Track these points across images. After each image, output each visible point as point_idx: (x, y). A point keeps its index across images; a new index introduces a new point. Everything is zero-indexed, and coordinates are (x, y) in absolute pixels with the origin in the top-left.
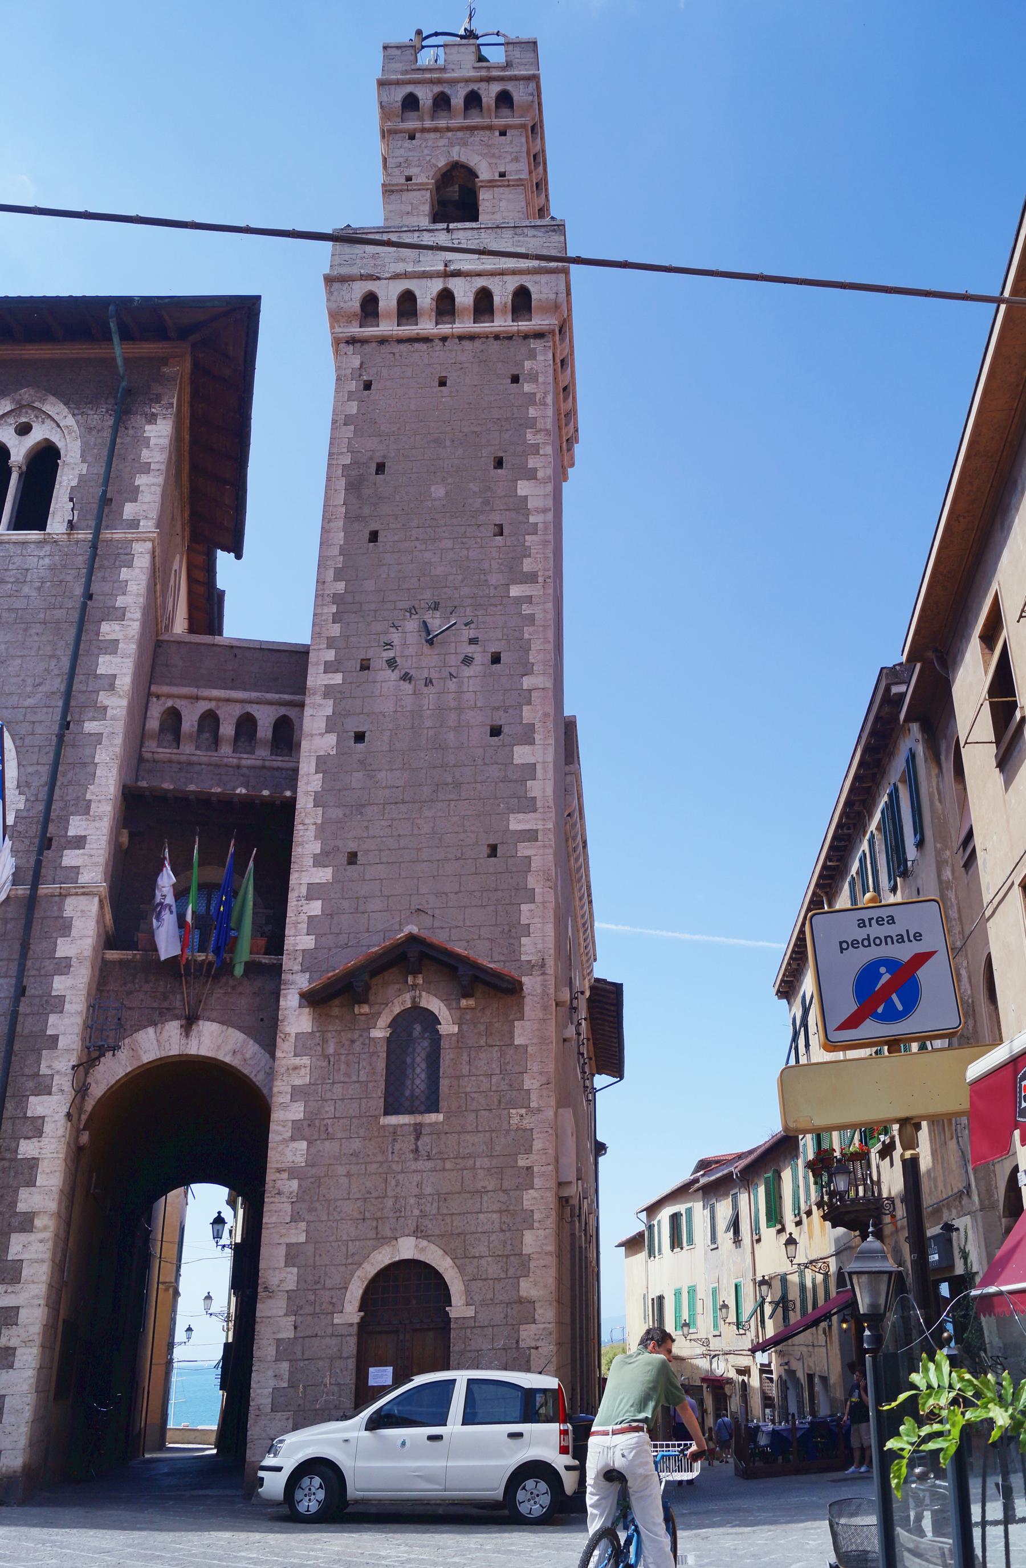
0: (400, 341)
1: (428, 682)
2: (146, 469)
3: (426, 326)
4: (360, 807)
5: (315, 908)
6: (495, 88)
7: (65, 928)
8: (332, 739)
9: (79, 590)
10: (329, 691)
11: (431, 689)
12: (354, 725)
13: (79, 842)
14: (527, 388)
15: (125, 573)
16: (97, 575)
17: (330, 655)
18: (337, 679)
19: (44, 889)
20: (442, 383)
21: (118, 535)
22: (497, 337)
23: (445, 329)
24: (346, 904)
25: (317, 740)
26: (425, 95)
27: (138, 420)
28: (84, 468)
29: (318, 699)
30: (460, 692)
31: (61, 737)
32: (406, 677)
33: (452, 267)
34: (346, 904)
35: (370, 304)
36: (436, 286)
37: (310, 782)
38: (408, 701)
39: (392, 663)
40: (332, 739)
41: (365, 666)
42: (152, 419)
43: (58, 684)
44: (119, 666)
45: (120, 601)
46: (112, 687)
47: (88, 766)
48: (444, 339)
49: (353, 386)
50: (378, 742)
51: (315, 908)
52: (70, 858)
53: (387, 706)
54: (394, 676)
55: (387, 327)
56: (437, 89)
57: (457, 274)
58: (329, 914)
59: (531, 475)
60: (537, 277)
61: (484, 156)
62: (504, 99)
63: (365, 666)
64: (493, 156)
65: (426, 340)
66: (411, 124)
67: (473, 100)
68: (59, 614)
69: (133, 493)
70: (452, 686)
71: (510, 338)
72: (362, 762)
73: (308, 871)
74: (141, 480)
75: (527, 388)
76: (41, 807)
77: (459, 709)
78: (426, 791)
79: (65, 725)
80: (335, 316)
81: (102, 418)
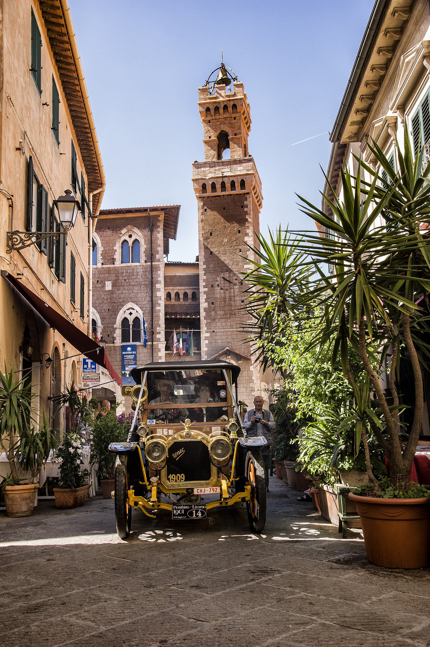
0: (213, 197)
1: (227, 290)
2: (159, 246)
3: (219, 192)
4: (214, 320)
5: (207, 342)
6: (232, 103)
7: (159, 350)
8: (207, 304)
9: (150, 277)
10: (205, 293)
11: (228, 292)
12: (210, 301)
13: (159, 333)
14: (246, 209)
15: (159, 272)
16: (153, 273)
17: (204, 284)
18: (206, 289)
19: (154, 343)
20: (224, 209)
21: (156, 263)
22: (237, 194)
23: (224, 193)
24: (213, 341)
25: (203, 305)
26: (212, 108)
27: (155, 233)
28: (146, 246)
29: (203, 294)
30: (234, 292)
31: (152, 311)
32: (221, 289)
33: (225, 175)
34: (213, 341)
35: (204, 187)
36: (220, 181)
37: (203, 314)
38: (223, 295)
39: (218, 285)
40: (207, 304)
41: (212, 286)
42: (159, 232)
43: (149, 299)
44: (161, 294)
45: (159, 279)
46: (161, 299)
47: (158, 316)
48: (224, 196)
49: (202, 211)
50: (217, 304)
51: (207, 342)
52: (158, 336)
53: (218, 296)
54: (219, 288)
55: (209, 193)
56: (215, 105)
57: (226, 177)
58: (210, 343)
59: (247, 235)
60: (246, 176)
61: (230, 127)
62: (234, 106)
63: (212, 286)
64: (233, 128)
65: (219, 196)
66: (209, 118)
67: (225, 107)
68: (147, 282)
69: (158, 252)
70: (232, 291)
71: (240, 194)
72: (214, 309)
73: (204, 334)
74: (159, 249)
75: (246, 209)
76: (150, 326)
77: (234, 296)
78: (228, 316)
79: (152, 308)
80: (196, 190)
81: (147, 232)
